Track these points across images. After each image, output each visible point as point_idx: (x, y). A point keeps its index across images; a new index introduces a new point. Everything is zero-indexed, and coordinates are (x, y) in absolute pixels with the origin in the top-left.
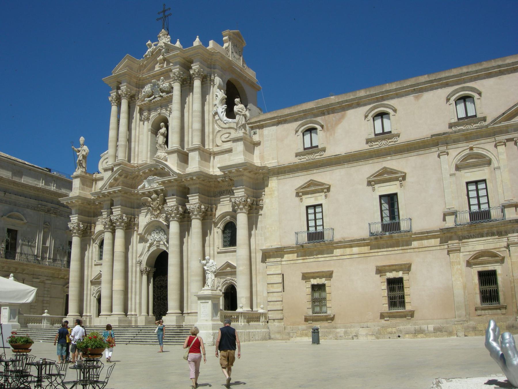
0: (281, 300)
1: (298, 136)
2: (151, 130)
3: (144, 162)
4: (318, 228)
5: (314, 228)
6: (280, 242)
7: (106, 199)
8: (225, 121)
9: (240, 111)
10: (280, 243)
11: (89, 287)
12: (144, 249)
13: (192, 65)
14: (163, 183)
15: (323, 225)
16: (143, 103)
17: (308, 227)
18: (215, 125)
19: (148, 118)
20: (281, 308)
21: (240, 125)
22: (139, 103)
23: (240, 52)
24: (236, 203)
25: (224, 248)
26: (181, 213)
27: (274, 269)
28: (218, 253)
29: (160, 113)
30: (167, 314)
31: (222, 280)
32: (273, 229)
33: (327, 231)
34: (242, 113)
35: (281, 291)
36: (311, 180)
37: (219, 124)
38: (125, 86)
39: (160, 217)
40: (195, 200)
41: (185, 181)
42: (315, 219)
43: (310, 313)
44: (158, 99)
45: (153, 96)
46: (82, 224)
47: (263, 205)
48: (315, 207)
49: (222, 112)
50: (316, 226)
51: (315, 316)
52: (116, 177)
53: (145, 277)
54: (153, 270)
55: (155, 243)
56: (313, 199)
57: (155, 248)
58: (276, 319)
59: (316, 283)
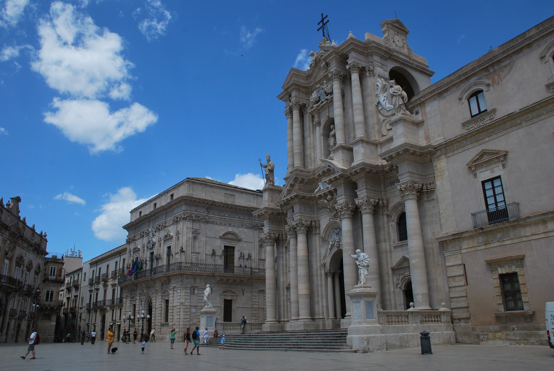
0: (465, 295)
1: (462, 104)
2: (323, 134)
3: (319, 165)
4: (499, 205)
5: (494, 206)
6: (457, 228)
7: (289, 206)
8: (388, 108)
9: (396, 93)
10: (457, 229)
11: (285, 294)
12: (326, 251)
13: (347, 61)
14: (330, 182)
15: (504, 201)
16: (312, 110)
17: (487, 205)
18: (380, 115)
19: (319, 123)
20: (466, 305)
21: (397, 107)
22: (309, 110)
23: (403, 40)
24: (402, 190)
25: (400, 242)
26: (352, 210)
27: (453, 260)
28: (395, 247)
29: (328, 116)
30: (346, 316)
31: (401, 277)
32: (448, 213)
33: (510, 206)
34: (398, 94)
35: (464, 285)
36: (483, 150)
37: (382, 113)
38: (295, 98)
39: (337, 217)
40: (363, 194)
41: (351, 176)
42: (495, 195)
43: (502, 309)
44: (325, 103)
45: (320, 102)
46: (274, 234)
47: (434, 188)
48: (492, 180)
49: (384, 100)
50: (496, 203)
51: (508, 313)
52: (292, 183)
53: (330, 280)
54: (338, 271)
55: (336, 243)
56: (488, 172)
57: (336, 250)
58: (463, 319)
59: (504, 272)
